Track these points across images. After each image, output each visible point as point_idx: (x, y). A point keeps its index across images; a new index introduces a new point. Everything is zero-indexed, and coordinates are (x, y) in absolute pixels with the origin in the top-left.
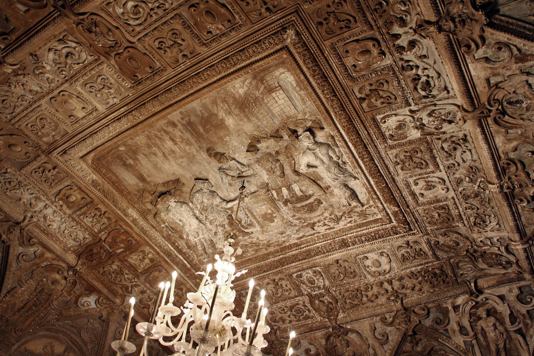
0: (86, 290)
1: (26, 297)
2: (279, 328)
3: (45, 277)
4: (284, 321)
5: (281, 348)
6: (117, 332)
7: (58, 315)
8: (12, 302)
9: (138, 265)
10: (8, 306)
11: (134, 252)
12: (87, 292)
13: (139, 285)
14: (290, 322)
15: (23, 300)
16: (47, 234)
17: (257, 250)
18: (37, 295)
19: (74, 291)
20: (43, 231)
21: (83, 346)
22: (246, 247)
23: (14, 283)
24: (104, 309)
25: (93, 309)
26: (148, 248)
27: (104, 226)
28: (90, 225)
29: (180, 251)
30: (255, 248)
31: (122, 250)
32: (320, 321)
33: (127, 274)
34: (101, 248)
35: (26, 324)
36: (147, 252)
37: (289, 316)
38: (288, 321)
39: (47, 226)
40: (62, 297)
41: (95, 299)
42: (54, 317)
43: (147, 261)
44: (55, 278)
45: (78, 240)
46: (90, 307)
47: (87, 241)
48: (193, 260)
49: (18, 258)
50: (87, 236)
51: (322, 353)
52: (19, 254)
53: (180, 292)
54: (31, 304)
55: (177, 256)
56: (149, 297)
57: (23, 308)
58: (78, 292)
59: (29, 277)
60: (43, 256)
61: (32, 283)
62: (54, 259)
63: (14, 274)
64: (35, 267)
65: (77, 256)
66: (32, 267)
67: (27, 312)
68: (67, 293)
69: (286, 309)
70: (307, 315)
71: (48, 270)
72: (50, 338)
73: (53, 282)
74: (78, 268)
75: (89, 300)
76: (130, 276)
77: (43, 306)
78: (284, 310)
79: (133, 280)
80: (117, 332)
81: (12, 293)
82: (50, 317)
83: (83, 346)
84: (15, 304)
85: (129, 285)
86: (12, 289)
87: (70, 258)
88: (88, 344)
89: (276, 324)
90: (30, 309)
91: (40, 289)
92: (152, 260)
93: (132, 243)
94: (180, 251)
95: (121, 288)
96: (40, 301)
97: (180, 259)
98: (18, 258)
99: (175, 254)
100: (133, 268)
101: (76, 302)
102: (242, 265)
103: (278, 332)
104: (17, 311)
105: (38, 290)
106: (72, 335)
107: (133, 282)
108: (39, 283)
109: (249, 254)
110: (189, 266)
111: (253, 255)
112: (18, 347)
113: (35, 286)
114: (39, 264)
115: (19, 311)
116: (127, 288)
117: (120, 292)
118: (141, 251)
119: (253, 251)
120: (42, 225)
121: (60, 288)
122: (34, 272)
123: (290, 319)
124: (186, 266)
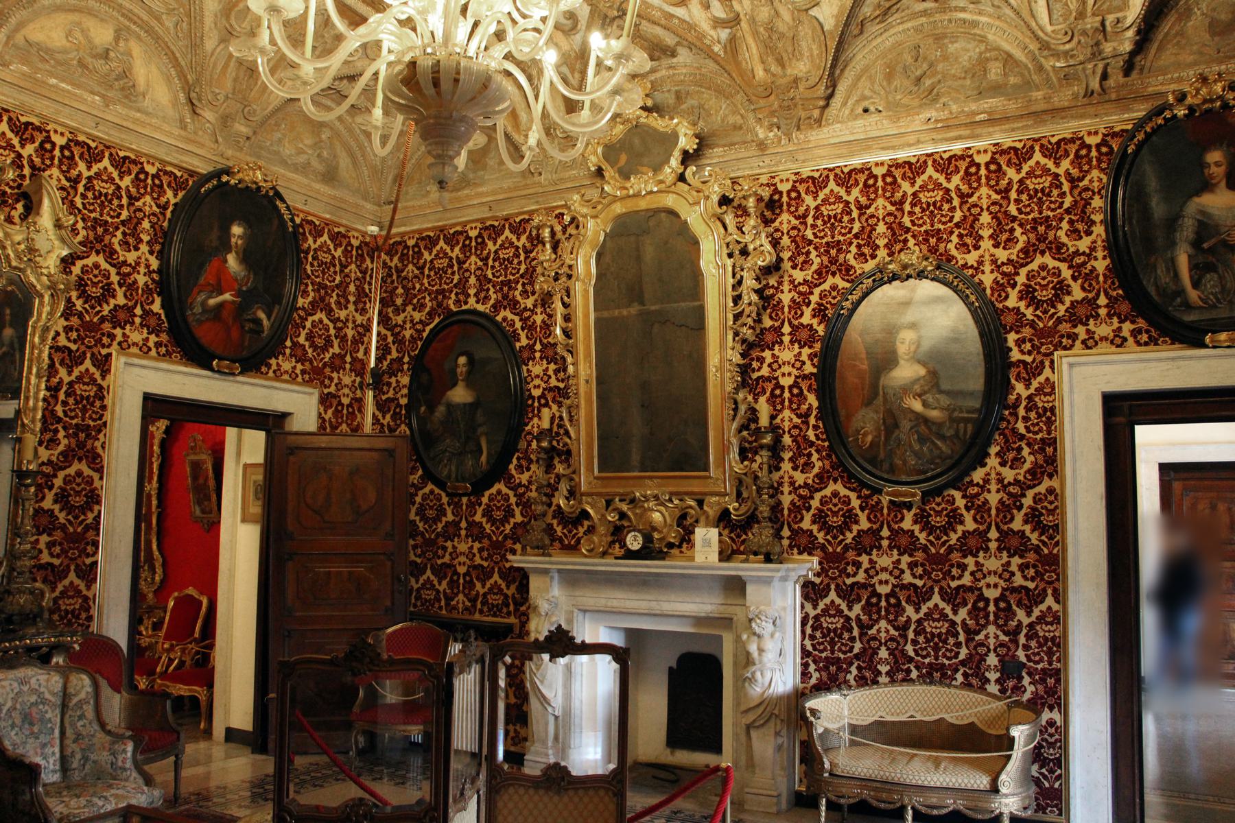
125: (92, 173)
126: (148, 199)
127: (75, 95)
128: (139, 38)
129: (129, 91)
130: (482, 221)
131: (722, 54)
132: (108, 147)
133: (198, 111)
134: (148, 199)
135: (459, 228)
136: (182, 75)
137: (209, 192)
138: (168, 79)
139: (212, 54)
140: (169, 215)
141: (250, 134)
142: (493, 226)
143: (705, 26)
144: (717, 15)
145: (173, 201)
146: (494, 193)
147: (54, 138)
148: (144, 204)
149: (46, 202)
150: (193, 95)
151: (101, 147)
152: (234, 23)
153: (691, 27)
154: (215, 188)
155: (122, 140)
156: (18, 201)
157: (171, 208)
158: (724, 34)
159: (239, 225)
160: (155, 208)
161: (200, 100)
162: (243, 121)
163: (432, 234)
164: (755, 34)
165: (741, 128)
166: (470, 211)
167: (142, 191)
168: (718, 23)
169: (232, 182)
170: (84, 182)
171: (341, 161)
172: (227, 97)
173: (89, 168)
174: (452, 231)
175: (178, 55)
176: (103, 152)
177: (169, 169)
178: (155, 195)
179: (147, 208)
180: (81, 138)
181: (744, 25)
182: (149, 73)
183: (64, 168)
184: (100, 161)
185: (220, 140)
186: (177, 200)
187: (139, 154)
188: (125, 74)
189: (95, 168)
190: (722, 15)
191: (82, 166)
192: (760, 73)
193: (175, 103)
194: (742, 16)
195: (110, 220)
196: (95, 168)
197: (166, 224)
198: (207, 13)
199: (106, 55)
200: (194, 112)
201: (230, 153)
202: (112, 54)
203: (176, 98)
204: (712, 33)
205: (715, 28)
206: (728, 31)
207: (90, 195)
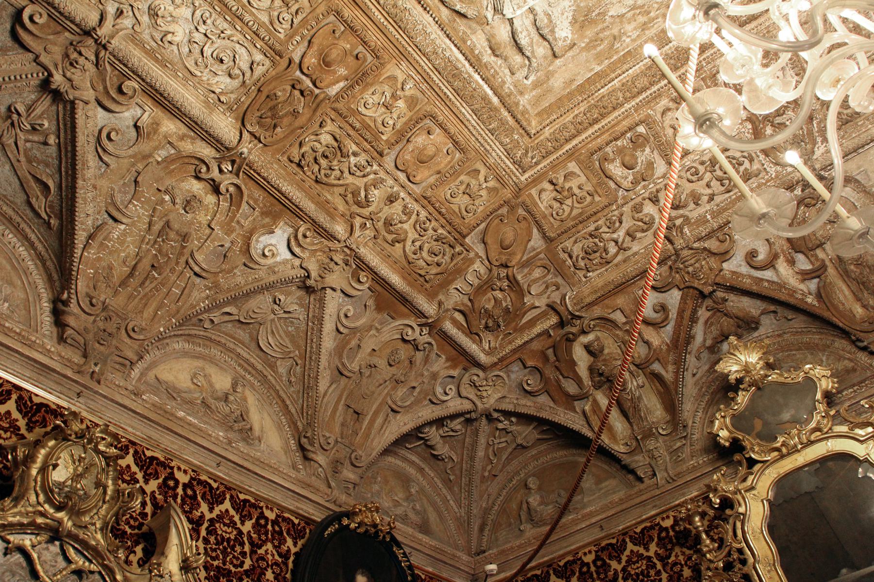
0: (264, 214)
1: (132, 249)
2: (687, 220)
3: (167, 192)
4: (696, 199)
5: (697, 265)
6: (342, 315)
7: (210, 289)
8: (104, 264)
9: (379, 120)
10: (96, 272)
11: (372, 85)
12: (267, 220)
13: (382, 181)
14: (711, 198)
15: (126, 257)
16: (163, 63)
17: (645, 24)
18: (155, 242)
19: (238, 222)
20: (151, 54)
21: (268, 372)
22: (621, 22)
23: (99, 213)
24: (309, 258)
25: (285, 262)
26: (404, 65)
27: (300, 17)
28: (265, 19)
29: (475, 62)
30: (641, 19)
31: (342, 84)
32: (777, 177)
33: (355, 154)
34: (293, 87)
35: (145, 315)
36: (401, 78)
37: (708, 186)
38: (706, 198)
39: (158, 37)
40: (214, 240)
41: (286, 236)
42: (203, 295)
43: (401, 104)
44: (189, 191)
45: (237, 72)
46: (278, 259)
47: (259, 71)
48: (504, 82)
49: (99, 140)
50: (258, 57)
51: (783, 250)
52: (100, 132)
53: (473, 182)
54: (146, 264)
55: (470, 76)
56: (405, 207)
57: (131, 275)
58: (247, 224)
59: (129, 197)
60: (156, 131)
61: (138, 211)
62: (182, 138)
63: (95, 187)
64: (140, 166)
65: (236, 119)
66: (133, 165)
67: (142, 284)
68: (222, 227)
69: (701, 169)
70: (746, 169)
71: (173, 171)
72: (197, 358)
73: (188, 202)
74: (245, 150)
75: (273, 241)
76: (362, 159)
77: (173, 270)
78: (696, 173)
79: (369, 169)
80: (342, 315)
81: (100, 238)
82: (195, 294)
83: (268, 372)
84: (111, 268)
85: (360, 183)
86: (98, 228)
87: (222, 125)
88: (278, 363)
89: (681, 212)
90: (146, 279)
91: (162, 224)
92: (412, 102)
93: (365, 60)
94: (475, 62)
95: (344, 196)
96: (167, 255)
97: (477, 82)
98: (99, 140)
99: (467, 73)
100: (368, 135)
101: (247, 250)
102: (614, 71)
103: (686, 230)
104: (120, 286)
105: (157, 228)
106: (239, 350)
107: (368, 174)
108: (154, 209)
109: (628, 40)
110: (495, 100)
111: (633, 41)
112: (142, 374)
113: (147, 220)
114: (150, 155)
115: (123, 283)
116: (355, 194)
117: (341, 207)
118: (389, 77)
119: (635, 29)
120: (146, 36)
121: (203, 218)
122: (140, 179)
123: (709, 191)
124: (490, 102)
125: (214, 515)
126: (269, 546)
127: (200, 430)
128: (252, 386)
129: (247, 434)
130: (596, 543)
131: (816, 303)
132: (229, 489)
133: (311, 455)
134: (269, 546)
135: (570, 558)
136: (293, 424)
137: (331, 535)
138: (279, 427)
139: (325, 394)
140: (291, 565)
141: (358, 480)
142: (611, 544)
143: (793, 281)
144: (803, 268)
145: (294, 550)
146: (604, 509)
147: (179, 475)
148: (266, 551)
149: (174, 539)
150: (304, 441)
151: (222, 488)
152: (345, 361)
153: (782, 286)
154: (336, 530)
155: (242, 482)
156: (137, 543)
157: (292, 558)
158: (813, 285)
159: (363, 574)
160: (277, 557)
161: (312, 444)
162: (350, 467)
163: (539, 572)
164: (845, 274)
165: (854, 370)
166: (578, 537)
167: (263, 537)
168: (805, 276)
169: (353, 526)
170: (206, 525)
171: (430, 515)
172: (336, 442)
173: (211, 510)
174: (562, 563)
175: (288, 402)
176: (224, 493)
177: (286, 515)
178: (276, 543)
179: (270, 557)
180: (204, 477)
181: (831, 271)
182: (262, 419)
183: (187, 508)
184: (222, 503)
185: (333, 484)
186: (297, 549)
187: (258, 498)
188: (242, 417)
189: (217, 511)
190: (809, 267)
191: (204, 507)
192: (859, 311)
193: (287, 450)
194: (828, 263)
195: (233, 570)
196: (217, 511)
197: (288, 576)
198: (323, 351)
199: (226, 398)
200: (306, 458)
201: (343, 498)
202: (231, 398)
203: (287, 443)
204: (802, 286)
205: (803, 281)
206: (816, 280)
207: (212, 539)
